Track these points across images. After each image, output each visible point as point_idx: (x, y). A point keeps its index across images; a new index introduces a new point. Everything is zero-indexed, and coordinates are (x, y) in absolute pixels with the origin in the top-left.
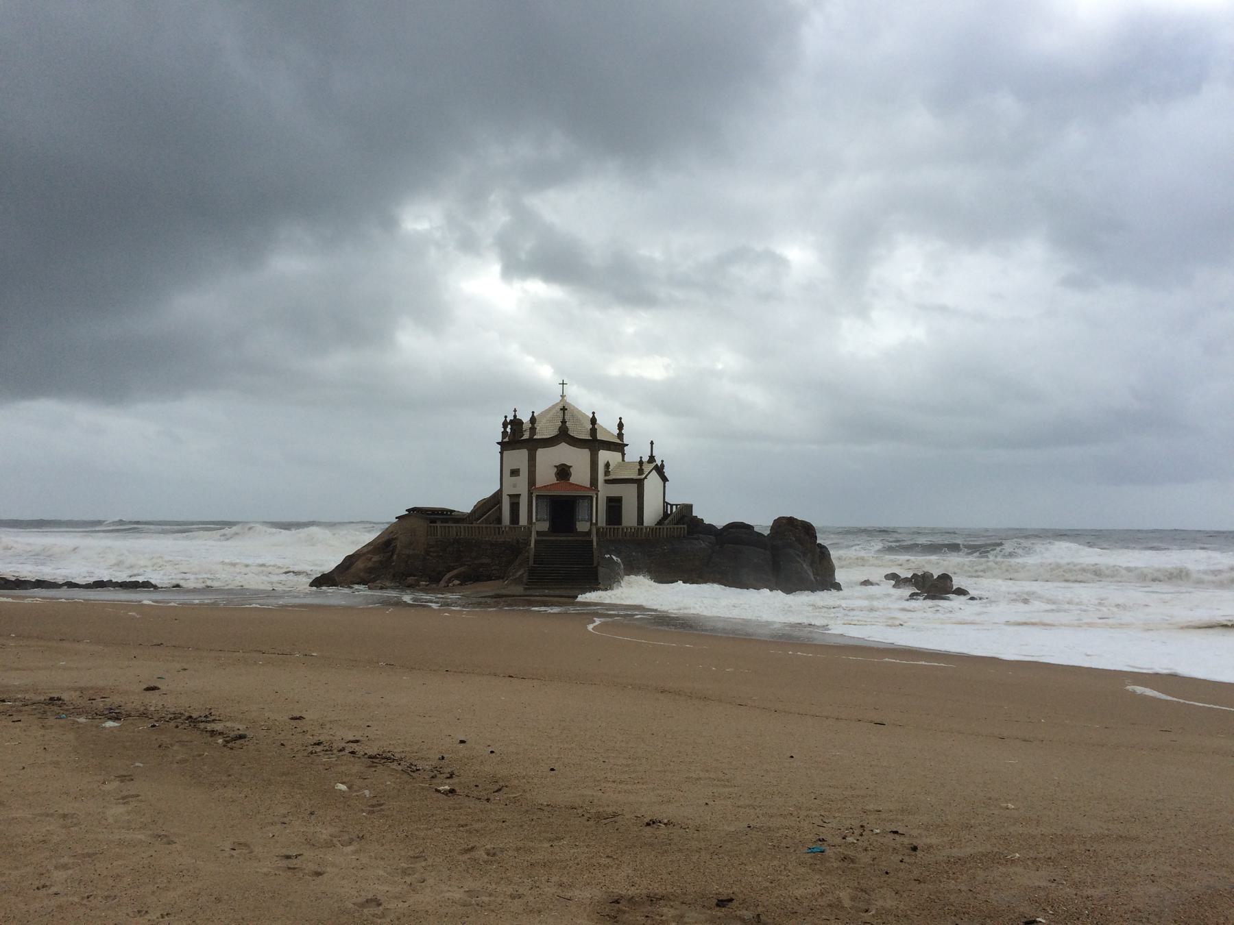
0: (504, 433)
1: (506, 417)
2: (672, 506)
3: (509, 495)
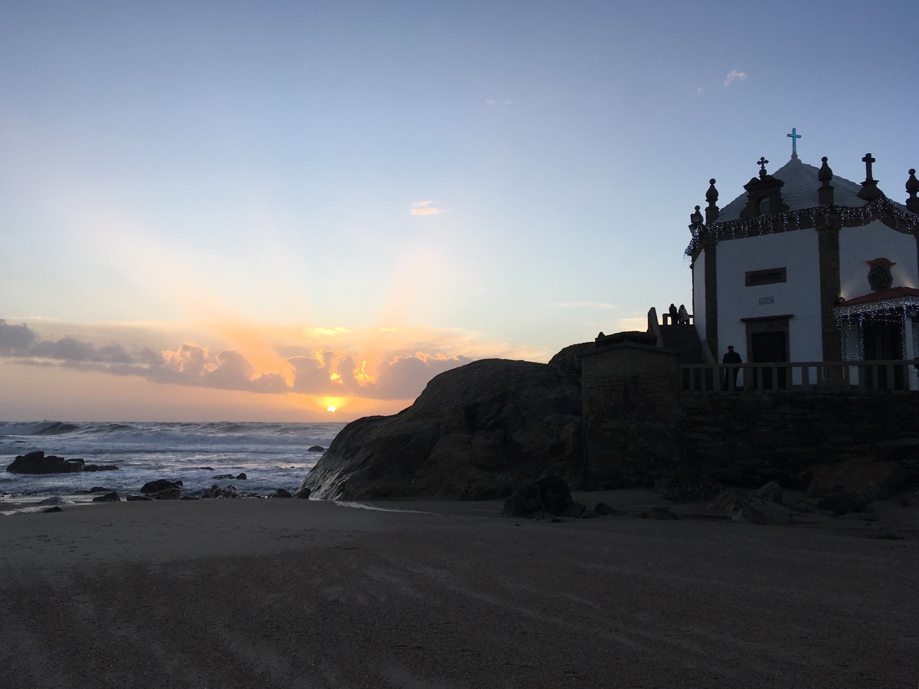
1: (713, 181)
3: (748, 321)
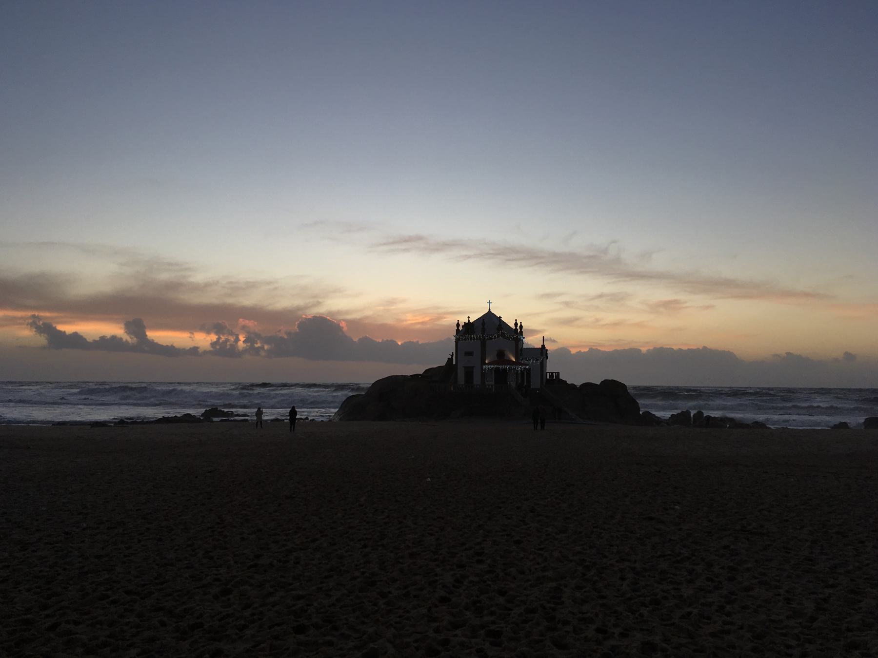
0: (458, 330)
1: (458, 321)
2: (547, 373)
